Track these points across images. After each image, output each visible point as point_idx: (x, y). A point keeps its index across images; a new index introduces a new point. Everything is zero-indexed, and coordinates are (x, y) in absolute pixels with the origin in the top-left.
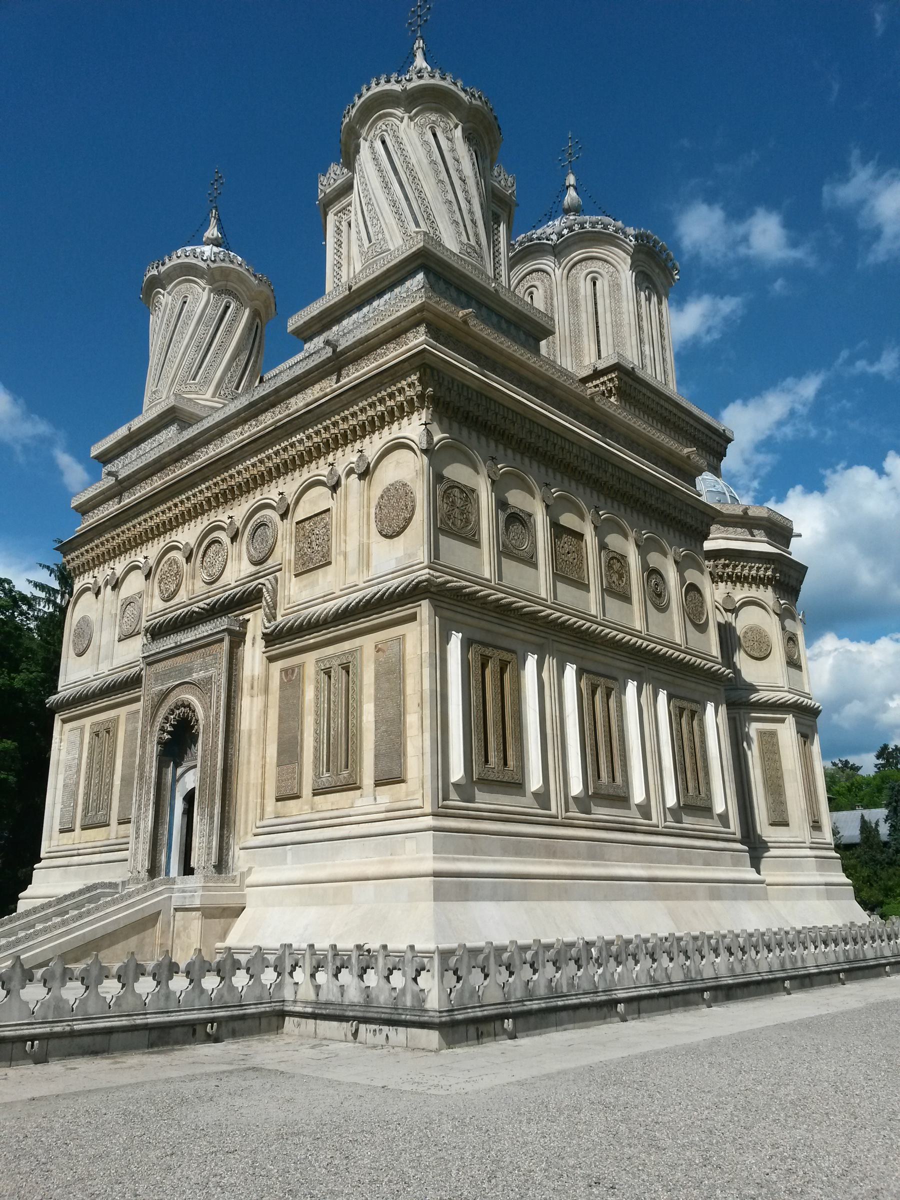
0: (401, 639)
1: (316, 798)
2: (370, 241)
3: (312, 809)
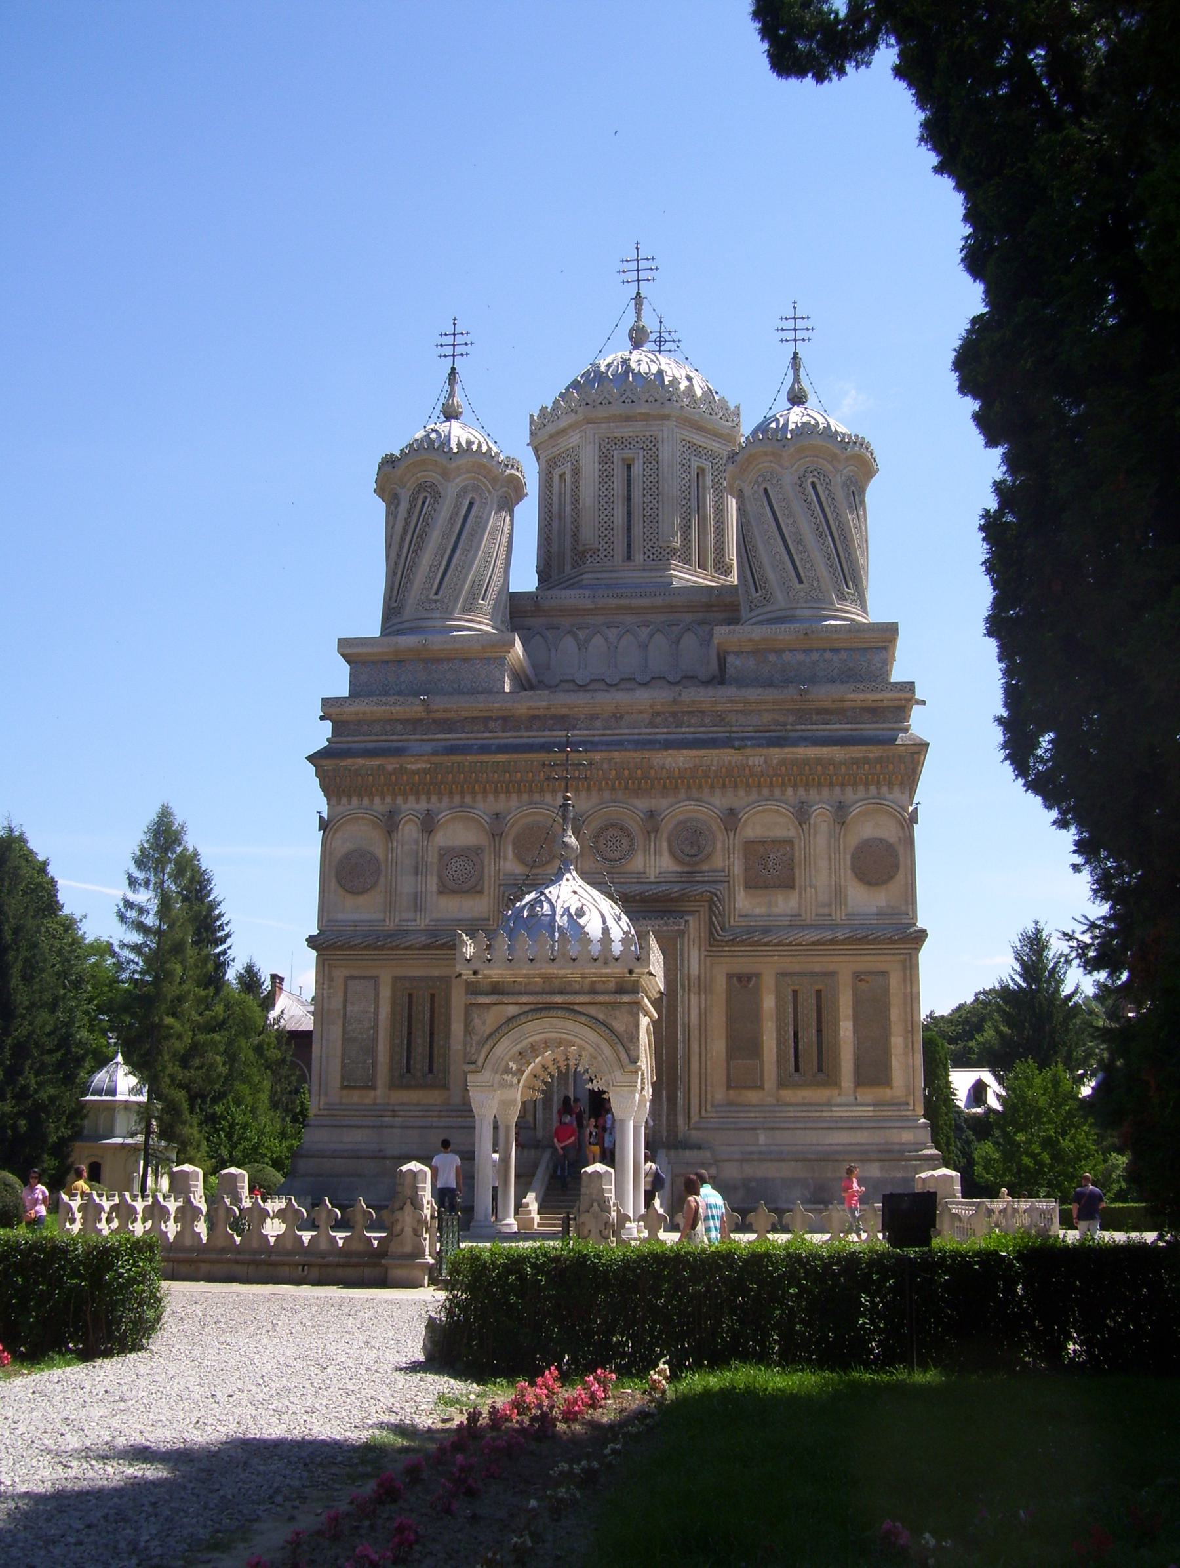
0: (884, 974)
2: (801, 582)
3: (778, 1101)
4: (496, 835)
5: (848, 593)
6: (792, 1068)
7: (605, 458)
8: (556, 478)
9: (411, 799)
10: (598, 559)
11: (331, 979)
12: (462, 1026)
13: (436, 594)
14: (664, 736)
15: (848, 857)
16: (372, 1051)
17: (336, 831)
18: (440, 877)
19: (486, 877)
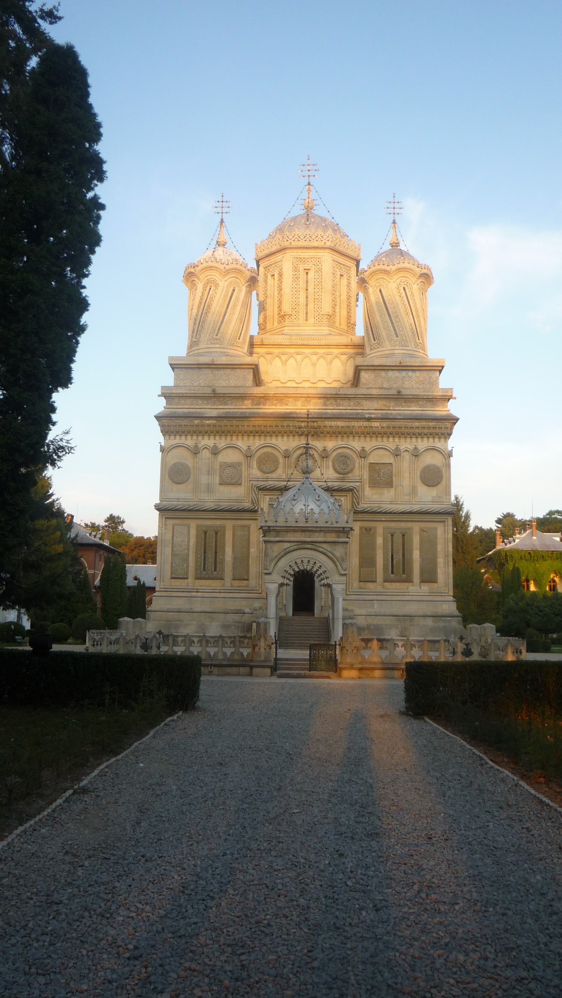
0: (436, 529)
1: (386, 584)
2: (397, 337)
4: (248, 456)
5: (420, 343)
6: (390, 572)
7: (296, 269)
8: (269, 277)
9: (206, 437)
10: (291, 320)
11: (166, 525)
12: (231, 549)
13: (217, 335)
14: (331, 411)
15: (419, 473)
16: (186, 560)
17: (169, 451)
18: (221, 477)
19: (243, 477)
